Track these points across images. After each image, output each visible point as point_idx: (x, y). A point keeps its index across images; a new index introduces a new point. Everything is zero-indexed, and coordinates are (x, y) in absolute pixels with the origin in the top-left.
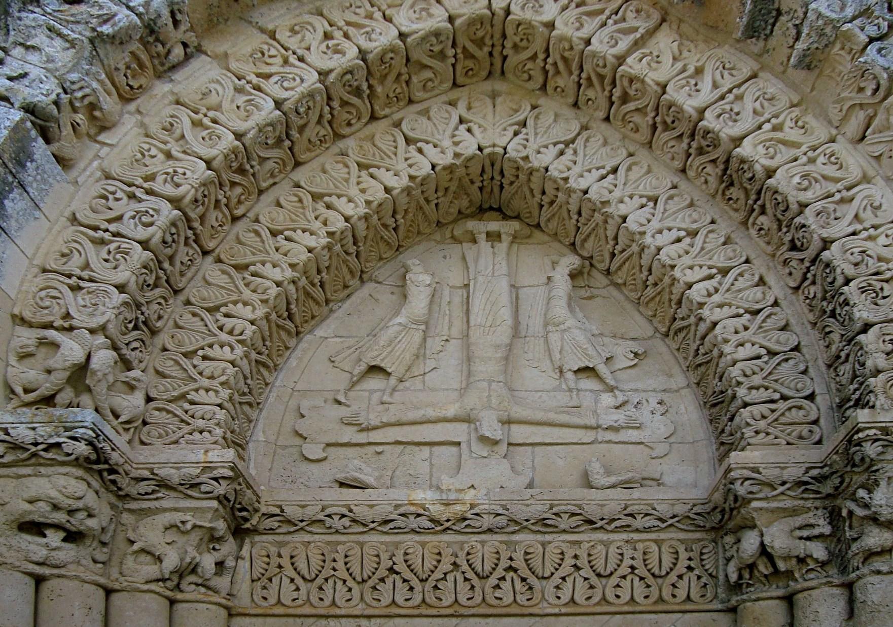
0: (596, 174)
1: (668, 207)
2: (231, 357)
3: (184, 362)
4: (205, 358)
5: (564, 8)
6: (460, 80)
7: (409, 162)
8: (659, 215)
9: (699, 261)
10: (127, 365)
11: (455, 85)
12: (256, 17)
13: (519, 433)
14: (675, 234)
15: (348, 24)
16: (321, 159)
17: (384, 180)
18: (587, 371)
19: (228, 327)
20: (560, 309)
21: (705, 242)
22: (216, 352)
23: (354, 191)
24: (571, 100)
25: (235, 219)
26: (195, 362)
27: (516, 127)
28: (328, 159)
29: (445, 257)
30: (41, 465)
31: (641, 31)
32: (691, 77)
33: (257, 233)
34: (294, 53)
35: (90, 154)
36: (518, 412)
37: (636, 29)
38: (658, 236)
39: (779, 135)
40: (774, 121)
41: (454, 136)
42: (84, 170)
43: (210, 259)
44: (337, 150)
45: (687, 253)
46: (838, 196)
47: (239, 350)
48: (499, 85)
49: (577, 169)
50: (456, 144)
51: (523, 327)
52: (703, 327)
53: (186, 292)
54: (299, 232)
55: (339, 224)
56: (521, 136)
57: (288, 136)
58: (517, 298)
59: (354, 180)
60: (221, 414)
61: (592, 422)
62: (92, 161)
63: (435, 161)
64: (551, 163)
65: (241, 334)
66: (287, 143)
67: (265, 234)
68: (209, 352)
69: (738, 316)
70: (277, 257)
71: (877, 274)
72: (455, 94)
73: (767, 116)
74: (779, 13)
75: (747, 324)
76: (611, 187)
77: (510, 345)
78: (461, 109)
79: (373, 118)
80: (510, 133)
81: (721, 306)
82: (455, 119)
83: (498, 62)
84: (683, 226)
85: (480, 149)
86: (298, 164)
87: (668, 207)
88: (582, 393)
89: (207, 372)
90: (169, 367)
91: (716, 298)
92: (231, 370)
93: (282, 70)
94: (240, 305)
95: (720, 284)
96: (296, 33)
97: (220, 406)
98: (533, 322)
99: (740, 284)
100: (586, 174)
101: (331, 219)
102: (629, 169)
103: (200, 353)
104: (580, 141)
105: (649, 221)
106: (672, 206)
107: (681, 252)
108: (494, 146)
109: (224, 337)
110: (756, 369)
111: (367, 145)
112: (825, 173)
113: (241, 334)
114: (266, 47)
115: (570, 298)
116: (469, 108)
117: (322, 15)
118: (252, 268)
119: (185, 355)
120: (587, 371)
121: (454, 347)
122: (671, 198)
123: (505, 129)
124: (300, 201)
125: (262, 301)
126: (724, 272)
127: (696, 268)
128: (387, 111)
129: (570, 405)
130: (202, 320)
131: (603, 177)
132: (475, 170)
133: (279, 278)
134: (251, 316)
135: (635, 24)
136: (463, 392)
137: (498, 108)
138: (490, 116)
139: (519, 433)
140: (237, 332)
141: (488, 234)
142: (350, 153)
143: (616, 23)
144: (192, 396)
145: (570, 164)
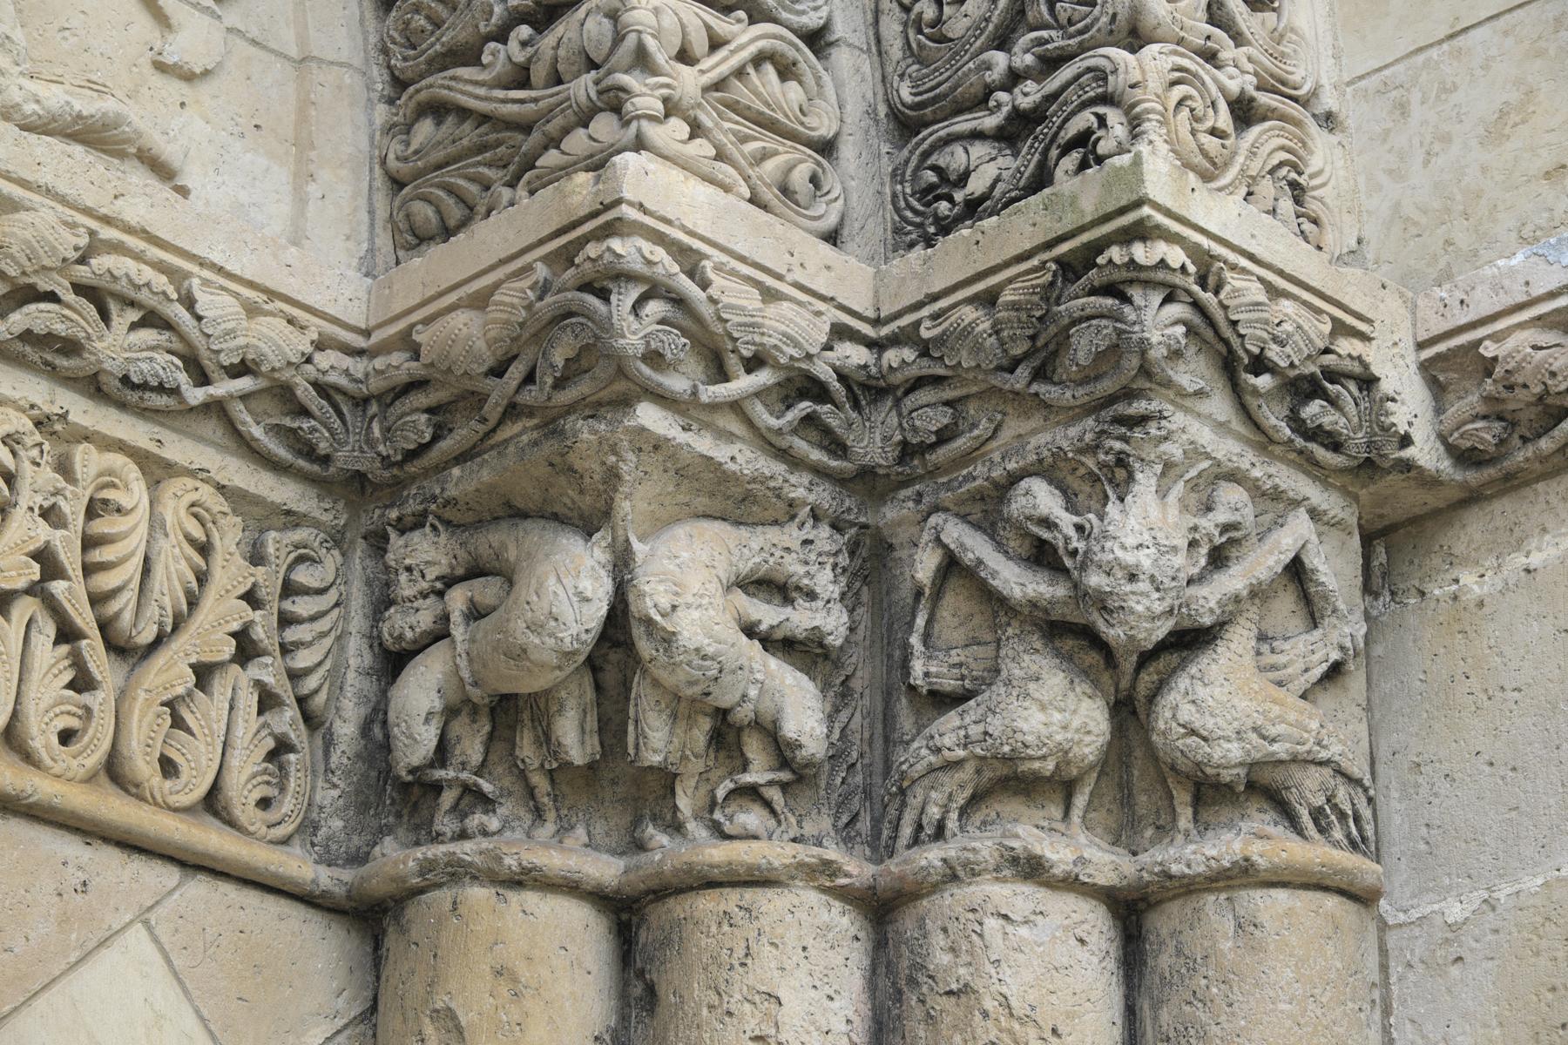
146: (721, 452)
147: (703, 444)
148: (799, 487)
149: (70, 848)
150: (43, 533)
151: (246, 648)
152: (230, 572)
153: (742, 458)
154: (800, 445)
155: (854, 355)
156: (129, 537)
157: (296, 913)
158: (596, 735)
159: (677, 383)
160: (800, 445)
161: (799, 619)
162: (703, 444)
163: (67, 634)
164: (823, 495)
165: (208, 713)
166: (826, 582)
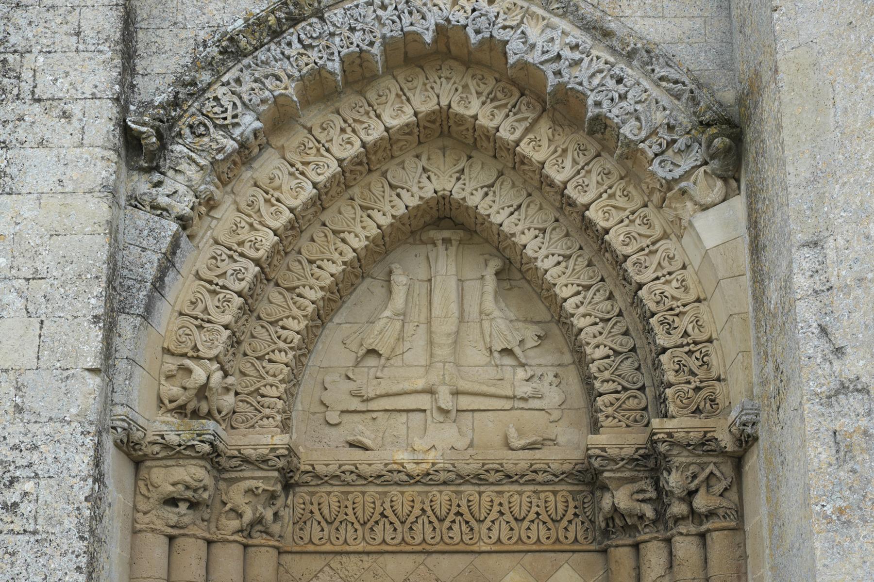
0: (508, 211)
1: (552, 236)
2: (285, 360)
3: (257, 363)
4: (270, 361)
5: (484, 103)
6: (422, 140)
7: (392, 204)
8: (546, 245)
9: (571, 280)
10: (226, 375)
11: (420, 143)
12: (302, 121)
13: (465, 402)
14: (557, 258)
15: (355, 121)
16: (338, 204)
17: (376, 219)
18: (507, 352)
19: (283, 338)
20: (489, 303)
21: (575, 264)
22: (277, 356)
23: (358, 229)
24: (492, 154)
25: (286, 254)
26: (264, 365)
27: (458, 175)
28: (342, 203)
29: (416, 256)
30: (180, 458)
31: (530, 120)
32: (560, 156)
33: (300, 262)
34: (323, 146)
35: (206, 224)
36: (463, 385)
37: (526, 119)
38: (546, 260)
39: (613, 202)
40: (609, 191)
41: (419, 182)
42: (202, 238)
43: (272, 284)
44: (348, 196)
45: (564, 273)
46: (647, 250)
47: (291, 354)
48: (448, 142)
49: (495, 208)
50: (421, 188)
51: (466, 314)
52: (575, 330)
53: (257, 311)
54: (325, 261)
55: (350, 255)
56: (461, 182)
57: (320, 199)
58: (463, 290)
59: (358, 219)
60: (280, 404)
61: (510, 393)
62: (205, 233)
63: (408, 204)
64: (479, 203)
65: (291, 342)
66: (319, 202)
67: (305, 263)
68: (272, 356)
69: (596, 324)
70: (312, 281)
71: (671, 309)
72: (418, 151)
73: (605, 187)
74: (606, 127)
75: (601, 330)
76: (517, 222)
77: (458, 332)
78: (424, 162)
79: (370, 171)
80: (454, 180)
81: (584, 316)
82: (420, 169)
83: (446, 128)
84: (562, 252)
85: (436, 192)
86: (324, 209)
87: (552, 236)
88: (504, 368)
89: (271, 372)
90: (250, 370)
91: (582, 310)
92: (286, 370)
93: (315, 159)
94: (290, 319)
95: (584, 298)
96: (324, 129)
97: (279, 398)
98: (473, 310)
99: (598, 298)
100: (501, 211)
101: (345, 251)
102: (528, 206)
104: (497, 185)
105: (540, 248)
106: (556, 236)
107: (560, 273)
108: (444, 190)
109: (282, 345)
110: (606, 366)
111: (366, 192)
112: (640, 232)
113: (291, 342)
114: (306, 140)
115: (496, 292)
116: (429, 159)
117: (339, 114)
118: (297, 291)
119: (257, 358)
120: (507, 352)
121: (423, 327)
122: (554, 229)
123: (451, 176)
124: (326, 236)
125: (303, 316)
126: (587, 288)
127: (570, 286)
128: (378, 166)
129: (497, 377)
130: (267, 330)
131: (512, 213)
132: (433, 204)
133: (314, 299)
134: (297, 328)
135: (526, 115)
136: (429, 366)
137: (447, 159)
138: (442, 167)
139: (465, 402)
140: (289, 340)
141: (443, 239)
142: (356, 199)
143: (515, 114)
145: (491, 203)
146: (623, 475)
147: (618, 475)
148: (641, 475)
149: (553, 555)
150: (537, 509)
151: (575, 515)
152: (572, 504)
153: (627, 474)
154: (638, 468)
155: (641, 452)
156: (551, 505)
157: (595, 554)
158: (618, 524)
159: (609, 468)
160: (638, 468)
161: (647, 496)
162: (618, 475)
163: (544, 523)
164: (647, 474)
165: (572, 528)
166: (650, 488)
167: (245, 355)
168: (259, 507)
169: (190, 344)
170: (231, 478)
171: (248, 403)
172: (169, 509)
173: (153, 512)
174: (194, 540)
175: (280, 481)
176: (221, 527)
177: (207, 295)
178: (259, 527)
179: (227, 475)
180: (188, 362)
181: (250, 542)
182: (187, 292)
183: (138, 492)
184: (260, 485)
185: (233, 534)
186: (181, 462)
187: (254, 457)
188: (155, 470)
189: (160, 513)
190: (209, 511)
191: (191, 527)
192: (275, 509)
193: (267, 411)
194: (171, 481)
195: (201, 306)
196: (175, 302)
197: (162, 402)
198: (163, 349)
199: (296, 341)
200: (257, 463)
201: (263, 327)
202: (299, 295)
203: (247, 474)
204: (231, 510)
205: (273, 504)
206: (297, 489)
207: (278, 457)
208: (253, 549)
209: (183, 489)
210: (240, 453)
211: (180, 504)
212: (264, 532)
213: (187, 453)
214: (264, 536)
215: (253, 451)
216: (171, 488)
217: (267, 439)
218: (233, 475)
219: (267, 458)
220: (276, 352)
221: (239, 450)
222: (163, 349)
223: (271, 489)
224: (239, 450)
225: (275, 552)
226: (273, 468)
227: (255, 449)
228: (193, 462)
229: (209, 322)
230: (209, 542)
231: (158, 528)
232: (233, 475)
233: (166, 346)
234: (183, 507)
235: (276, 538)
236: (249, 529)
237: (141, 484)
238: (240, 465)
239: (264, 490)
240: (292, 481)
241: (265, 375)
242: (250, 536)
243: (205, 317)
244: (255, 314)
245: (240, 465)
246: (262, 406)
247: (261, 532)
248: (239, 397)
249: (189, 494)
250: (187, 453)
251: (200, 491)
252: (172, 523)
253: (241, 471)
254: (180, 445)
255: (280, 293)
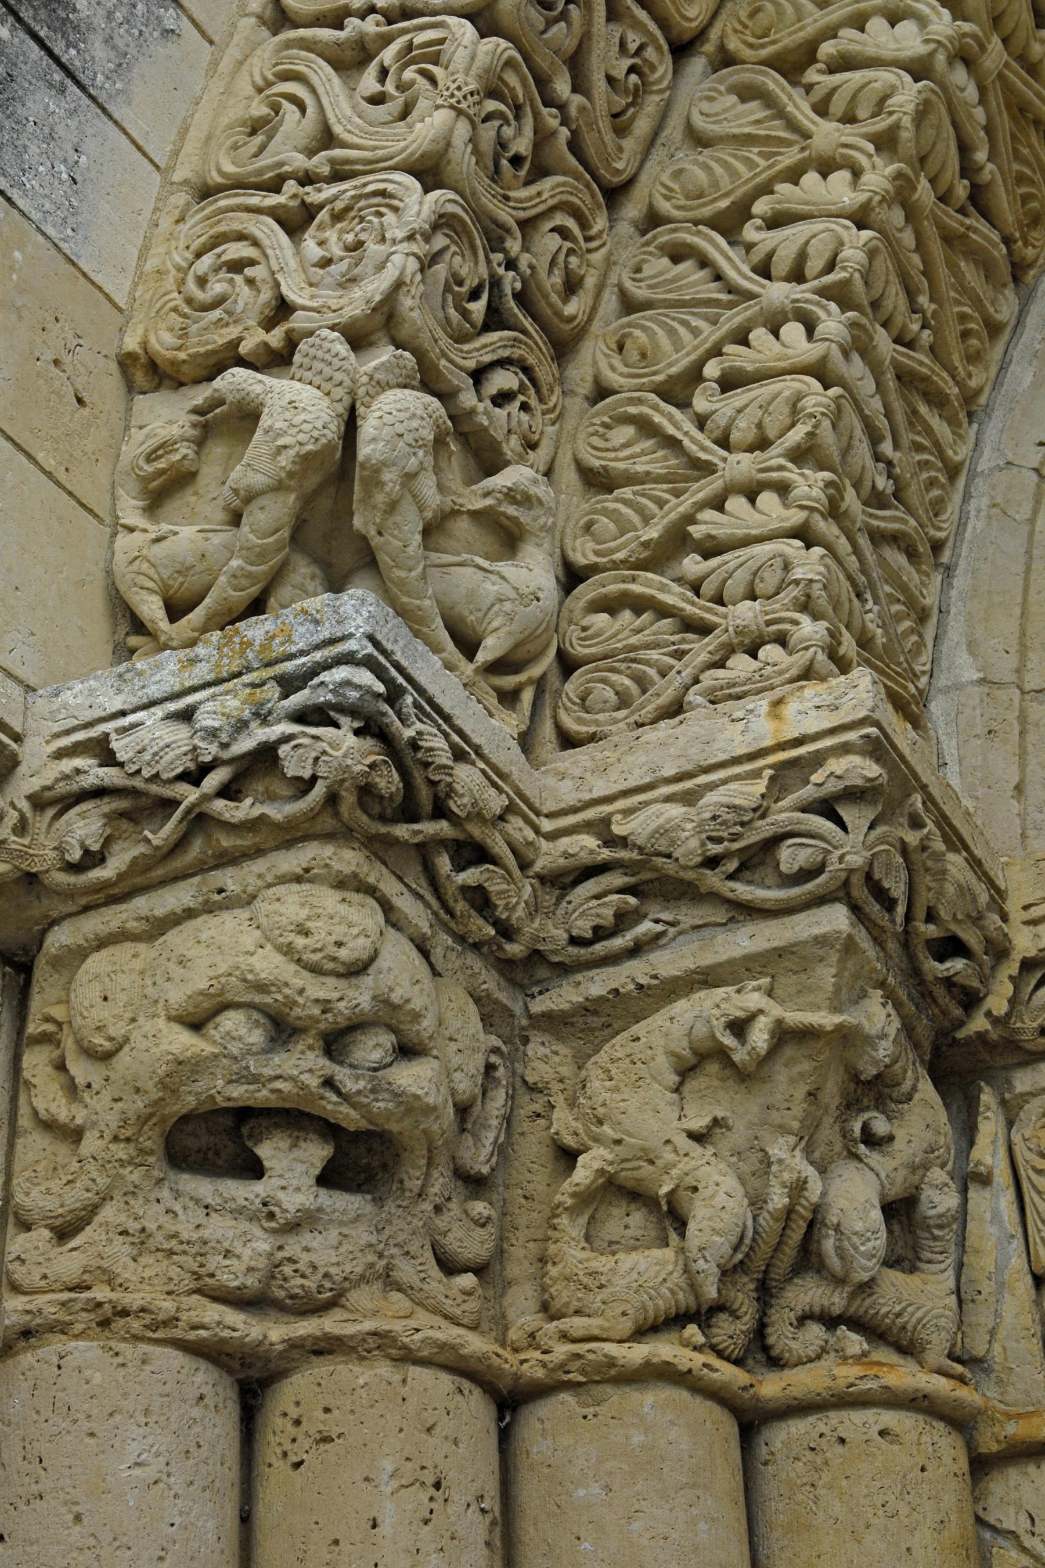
4: (728, 383)
19: (782, 264)
65: (831, 266)
68: (737, 357)
89: (743, 431)
90: (627, 452)
92: (817, 398)
103: (712, 369)
109: (778, 293)
113: (831, 266)
140: (814, 265)
144: (709, 525)
167: (601, 392)
168: (779, 1149)
169: (248, 301)
170: (591, 1008)
171: (640, 605)
172: (204, 1187)
173: (108, 1213)
174: (384, 1369)
175: (890, 996)
176: (563, 1295)
177: (322, 73)
178: (808, 1293)
179: (564, 996)
180: (237, 378)
181: (771, 1387)
182: (228, 91)
183: (24, 1121)
184: (754, 1000)
185: (643, 1332)
186: (231, 879)
187: (690, 846)
188: (97, 962)
189: (153, 1218)
190: (480, 1208)
191: (360, 1298)
192: (887, 1168)
193: (745, 613)
194: (177, 996)
195: (295, 128)
196: (176, 153)
197: (139, 627)
198: (126, 362)
199: (853, 255)
200: (713, 880)
201: (677, 254)
202: (844, 63)
203: (667, 963)
204: (618, 1190)
205: (870, 1139)
206: (1023, 1081)
207: (827, 808)
208: (798, 1427)
209: (257, 1037)
210: (611, 841)
211: (269, 1151)
212: (857, 1324)
213: (245, 809)
214: (854, 1342)
215: (675, 811)
216: (183, 1041)
217: (755, 726)
218: (597, 984)
219: (764, 829)
220: (759, 335)
221: (601, 828)
222: (126, 362)
223: (826, 1020)
224: (601, 828)
225: (948, 1450)
226: (812, 885)
227: (689, 798)
228: (291, 861)
229: (338, 176)
230: (510, 1401)
231: (133, 1300)
232: (597, 984)
233: (131, 343)
234: (291, 1168)
235: (936, 1355)
236: (744, 1299)
237: (36, 1062)
238: (623, 919)
239: (785, 1036)
240: (979, 1023)
241: (715, 454)
242: (759, 1350)
243: (320, 163)
244: (632, 210)
245: (623, 919)
246: (719, 600)
247: (831, 1322)
248: (587, 592)
249: (301, 1067)
250: (245, 809)
251: (373, 1047)
252: (231, 1275)
253: (635, 950)
254: (194, 776)
255: (746, 93)
